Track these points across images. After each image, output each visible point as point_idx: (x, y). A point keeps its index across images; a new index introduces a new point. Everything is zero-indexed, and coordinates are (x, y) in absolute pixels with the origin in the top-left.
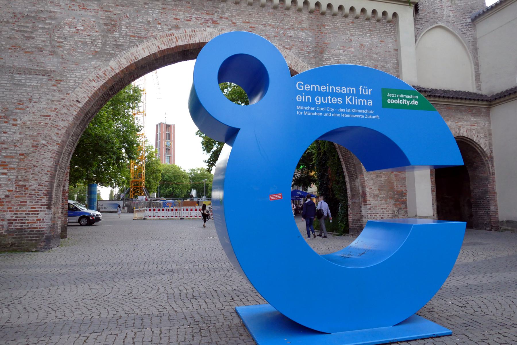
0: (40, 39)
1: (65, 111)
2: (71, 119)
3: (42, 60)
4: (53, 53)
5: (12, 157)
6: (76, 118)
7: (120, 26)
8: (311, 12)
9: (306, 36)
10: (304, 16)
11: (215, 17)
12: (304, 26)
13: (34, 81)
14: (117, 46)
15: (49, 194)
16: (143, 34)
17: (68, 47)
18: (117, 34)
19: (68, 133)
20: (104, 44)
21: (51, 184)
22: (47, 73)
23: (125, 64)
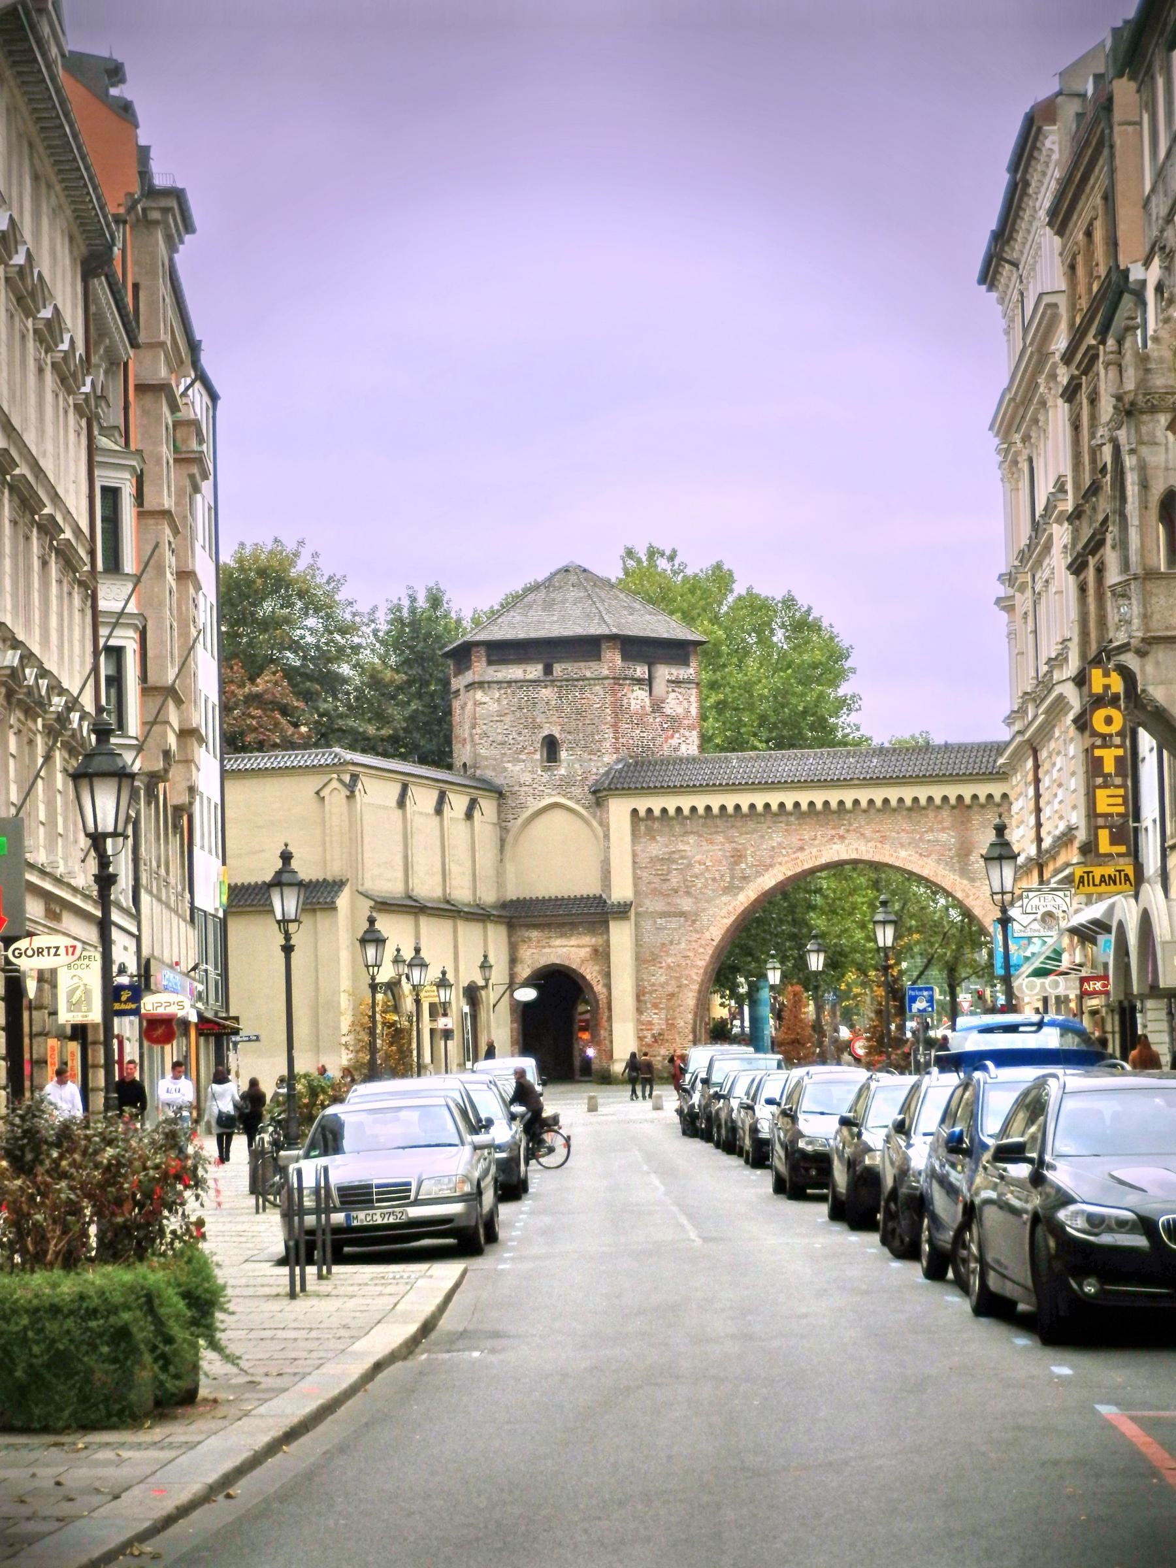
0: (675, 880)
1: (701, 950)
2: (708, 958)
3: (678, 901)
4: (688, 893)
5: (661, 998)
6: (712, 957)
7: (745, 857)
8: (953, 807)
9: (948, 837)
10: (945, 813)
11: (842, 831)
12: (946, 824)
13: (674, 923)
14: (744, 878)
15: (694, 1031)
16: (768, 861)
17: (700, 885)
18: (743, 866)
19: (705, 973)
20: (732, 878)
21: (695, 1021)
22: (682, 914)
23: (753, 896)
